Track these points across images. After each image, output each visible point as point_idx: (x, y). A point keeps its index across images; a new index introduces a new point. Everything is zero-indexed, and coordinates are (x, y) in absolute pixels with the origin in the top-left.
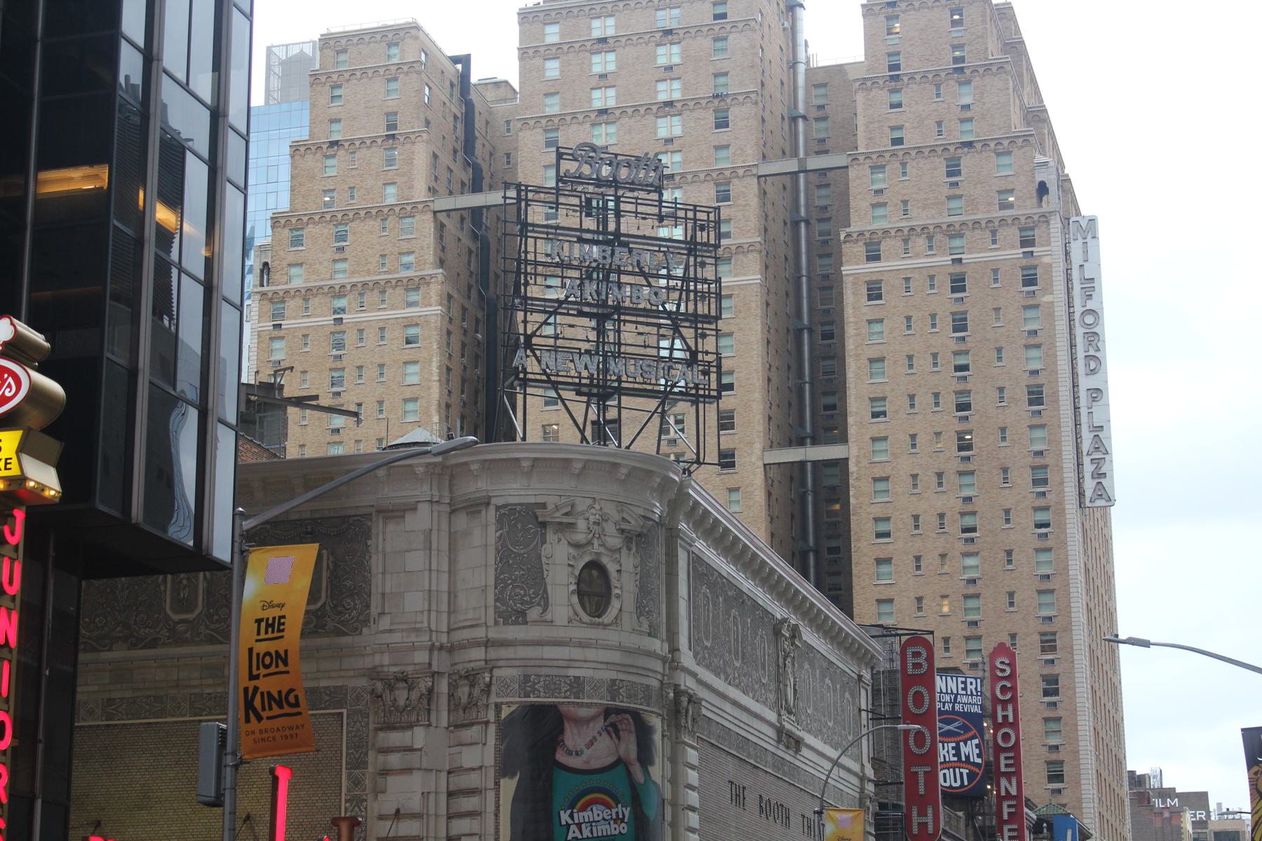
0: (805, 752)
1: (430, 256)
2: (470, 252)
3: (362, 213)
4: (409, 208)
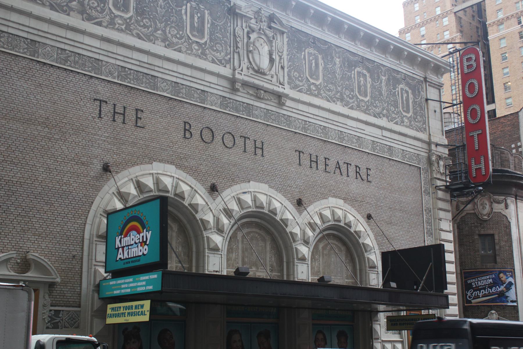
0: (289, 103)
1: (454, 29)
2: (477, 28)
3: (429, 21)
4: (445, 14)
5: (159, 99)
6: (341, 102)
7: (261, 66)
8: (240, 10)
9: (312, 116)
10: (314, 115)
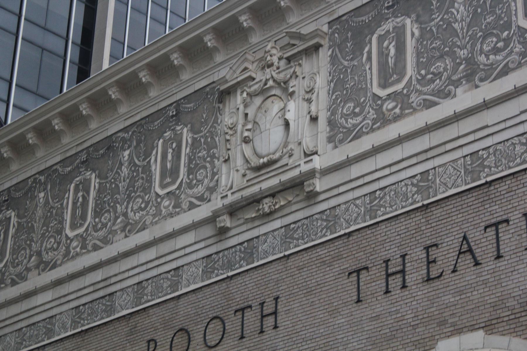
0: (319, 185)
5: (117, 324)
6: (468, 81)
7: (264, 153)
8: (227, 82)
9: (387, 171)
10: (390, 166)
